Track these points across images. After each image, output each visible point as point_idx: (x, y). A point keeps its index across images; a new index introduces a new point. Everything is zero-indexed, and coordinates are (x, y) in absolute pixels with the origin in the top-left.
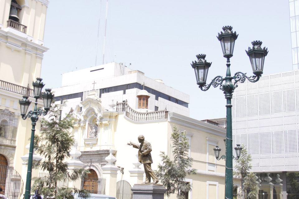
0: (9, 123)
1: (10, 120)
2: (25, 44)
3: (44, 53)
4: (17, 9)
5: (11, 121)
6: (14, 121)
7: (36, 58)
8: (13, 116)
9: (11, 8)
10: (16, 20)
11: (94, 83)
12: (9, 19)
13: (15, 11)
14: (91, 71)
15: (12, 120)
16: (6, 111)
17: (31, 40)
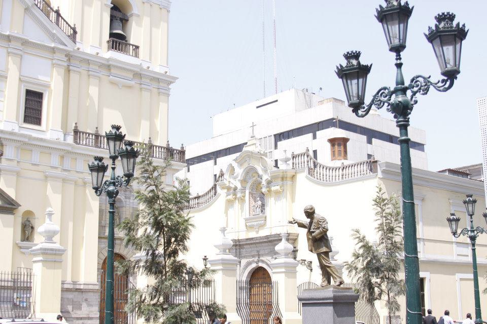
0: (124, 202)
2: (138, 74)
3: (170, 87)
5: (128, 200)
7: (159, 95)
8: (131, 192)
9: (111, 21)
10: (122, 37)
11: (253, 126)
12: (110, 38)
13: (118, 23)
14: (258, 107)
17: (148, 68)
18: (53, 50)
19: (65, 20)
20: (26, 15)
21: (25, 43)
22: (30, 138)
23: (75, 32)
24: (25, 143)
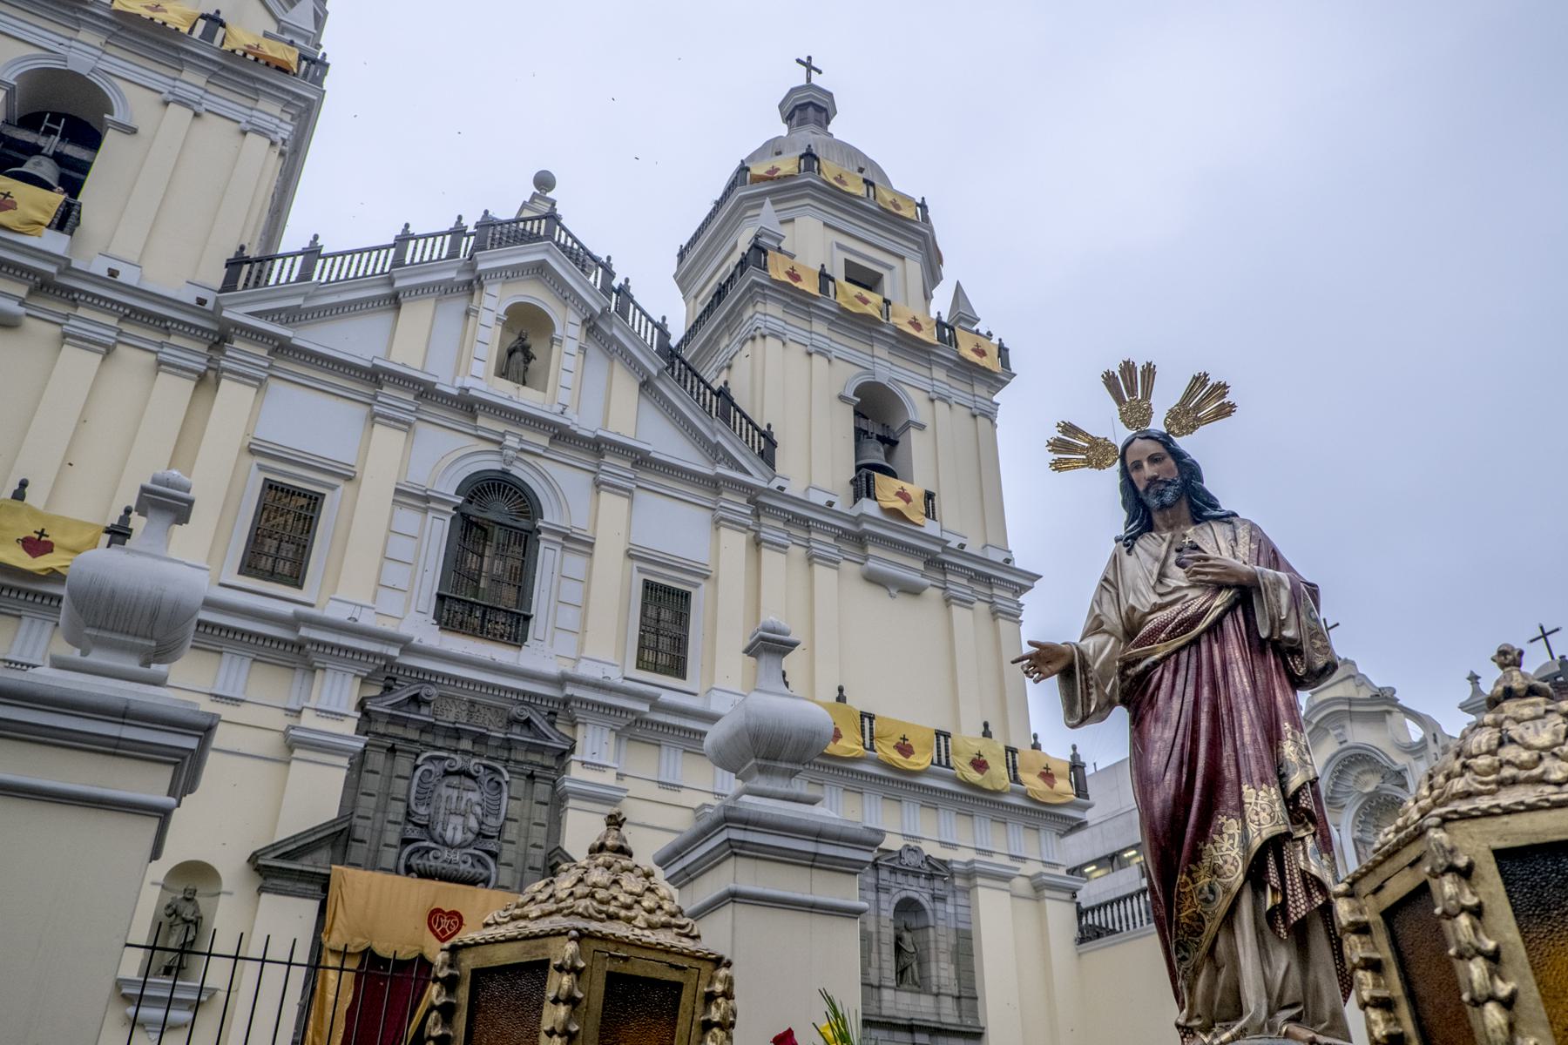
0: (930, 913)
1: (934, 898)
3: (1021, 599)
4: (883, 440)
5: (939, 906)
6: (950, 900)
9: (857, 440)
15: (943, 899)
17: (962, 546)
18: (714, 484)
19: (744, 415)
20: (643, 400)
21: (642, 460)
22: (656, 705)
23: (772, 444)
24: (640, 721)
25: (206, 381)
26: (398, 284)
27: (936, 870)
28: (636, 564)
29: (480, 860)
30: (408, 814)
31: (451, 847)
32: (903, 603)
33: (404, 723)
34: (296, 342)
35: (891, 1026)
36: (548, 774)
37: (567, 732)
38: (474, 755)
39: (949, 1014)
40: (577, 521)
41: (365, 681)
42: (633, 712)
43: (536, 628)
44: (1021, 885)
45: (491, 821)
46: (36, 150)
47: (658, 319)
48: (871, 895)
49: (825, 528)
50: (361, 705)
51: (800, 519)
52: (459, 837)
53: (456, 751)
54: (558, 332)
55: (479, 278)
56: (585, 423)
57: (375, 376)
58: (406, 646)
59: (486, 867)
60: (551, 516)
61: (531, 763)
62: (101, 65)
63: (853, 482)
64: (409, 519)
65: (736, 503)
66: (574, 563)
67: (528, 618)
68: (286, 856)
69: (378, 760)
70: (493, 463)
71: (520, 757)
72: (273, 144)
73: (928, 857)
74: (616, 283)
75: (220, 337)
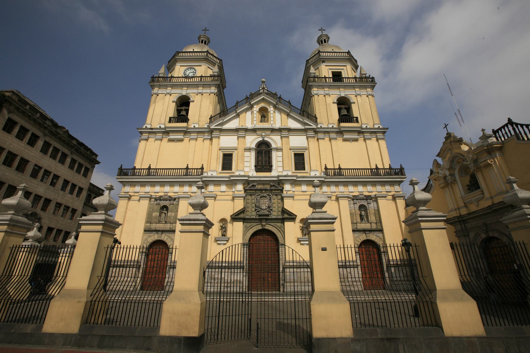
0: (367, 207)
1: (368, 204)
2: (360, 132)
5: (369, 205)
6: (372, 203)
11: (446, 126)
15: (370, 203)
16: (362, 196)
18: (305, 130)
20: (288, 118)
21: (289, 130)
22: (298, 177)
24: (295, 180)
25: (211, 139)
26: (238, 112)
27: (368, 198)
28: (292, 150)
29: (269, 211)
30: (255, 205)
31: (264, 210)
32: (354, 143)
33: (252, 190)
34: (223, 128)
35: (359, 231)
36: (280, 194)
37: (282, 186)
38: (265, 193)
39: (374, 226)
40: (279, 145)
41: (244, 184)
42: (293, 179)
43: (274, 167)
44: (391, 197)
45: (270, 204)
46: (182, 110)
47: (288, 101)
48: (352, 205)
49: (333, 132)
50: (244, 188)
51: (327, 132)
52: (264, 208)
53: (262, 193)
54: (269, 110)
55: (252, 105)
56: (278, 126)
57: (237, 130)
58: (249, 177)
59: (270, 212)
60: (273, 146)
61: (276, 193)
62: (187, 92)
63: (339, 120)
64: (247, 154)
65: (311, 133)
66: (280, 154)
67: (272, 166)
68: (236, 216)
69: (249, 197)
70: (261, 139)
71: (274, 192)
72: (215, 94)
73: (365, 195)
74: (278, 97)
75: (211, 131)
